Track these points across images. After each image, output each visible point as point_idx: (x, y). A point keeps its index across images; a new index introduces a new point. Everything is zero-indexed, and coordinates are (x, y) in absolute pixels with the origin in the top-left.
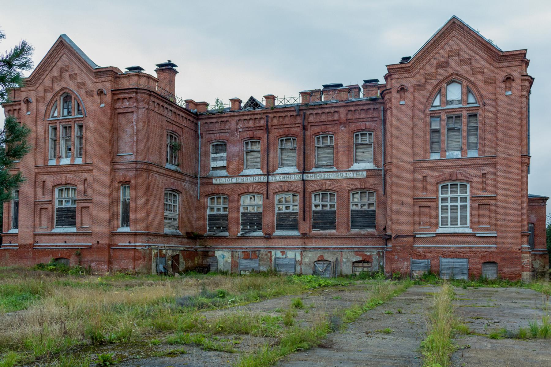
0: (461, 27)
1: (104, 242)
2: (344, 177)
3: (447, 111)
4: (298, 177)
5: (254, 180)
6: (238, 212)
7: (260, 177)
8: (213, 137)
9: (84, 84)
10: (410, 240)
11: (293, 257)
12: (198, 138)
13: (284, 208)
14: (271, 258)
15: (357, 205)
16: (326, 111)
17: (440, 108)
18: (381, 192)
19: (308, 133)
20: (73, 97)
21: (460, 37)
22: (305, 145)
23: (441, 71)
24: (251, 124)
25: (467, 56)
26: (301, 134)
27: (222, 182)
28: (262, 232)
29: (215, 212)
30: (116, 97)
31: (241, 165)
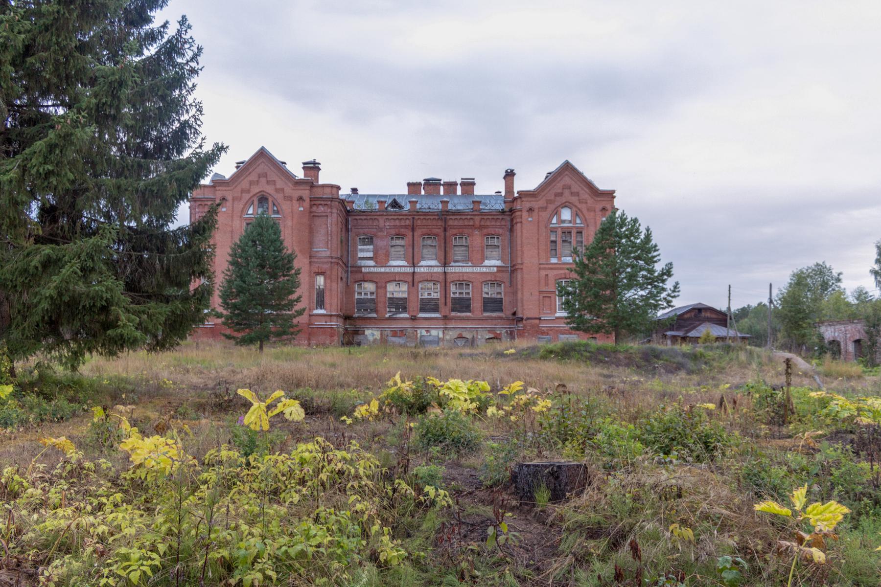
1: (304, 322)
2: (478, 271)
3: (562, 228)
4: (440, 270)
6: (386, 296)
8: (361, 231)
9: (282, 190)
10: (537, 321)
11: (436, 334)
13: (426, 294)
14: (417, 336)
15: (488, 293)
16: (464, 217)
17: (557, 226)
18: (508, 284)
19: (448, 234)
20: (270, 199)
22: (445, 243)
23: (558, 198)
24: (397, 223)
25: (576, 191)
26: (442, 234)
29: (363, 297)
30: (312, 203)
31: (388, 257)
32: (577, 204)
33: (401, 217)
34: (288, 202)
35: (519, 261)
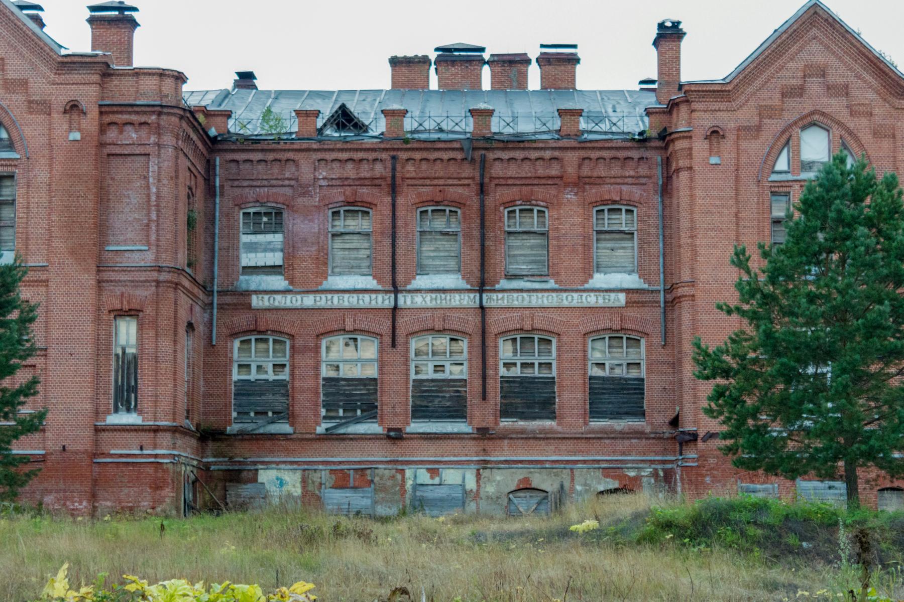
0: (829, 23)
1: (80, 447)
2: (575, 303)
4: (468, 300)
5: (361, 302)
7: (374, 296)
8: (250, 194)
9: (24, 83)
12: (214, 196)
13: (431, 367)
15: (601, 365)
16: (534, 155)
17: (790, 177)
18: (657, 340)
19: (490, 201)
21: (826, 41)
22: (483, 226)
23: (790, 103)
24: (350, 171)
25: (840, 81)
26: (475, 201)
27: (276, 304)
28: (376, 425)
29: (253, 376)
30: (107, 119)
32: (845, 117)
33: (360, 155)
34: (41, 118)
35: (686, 276)
